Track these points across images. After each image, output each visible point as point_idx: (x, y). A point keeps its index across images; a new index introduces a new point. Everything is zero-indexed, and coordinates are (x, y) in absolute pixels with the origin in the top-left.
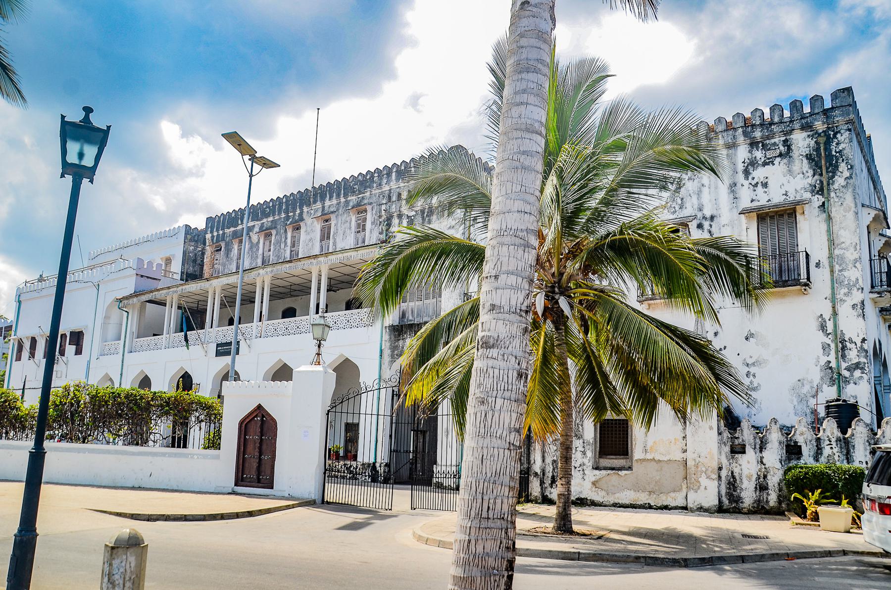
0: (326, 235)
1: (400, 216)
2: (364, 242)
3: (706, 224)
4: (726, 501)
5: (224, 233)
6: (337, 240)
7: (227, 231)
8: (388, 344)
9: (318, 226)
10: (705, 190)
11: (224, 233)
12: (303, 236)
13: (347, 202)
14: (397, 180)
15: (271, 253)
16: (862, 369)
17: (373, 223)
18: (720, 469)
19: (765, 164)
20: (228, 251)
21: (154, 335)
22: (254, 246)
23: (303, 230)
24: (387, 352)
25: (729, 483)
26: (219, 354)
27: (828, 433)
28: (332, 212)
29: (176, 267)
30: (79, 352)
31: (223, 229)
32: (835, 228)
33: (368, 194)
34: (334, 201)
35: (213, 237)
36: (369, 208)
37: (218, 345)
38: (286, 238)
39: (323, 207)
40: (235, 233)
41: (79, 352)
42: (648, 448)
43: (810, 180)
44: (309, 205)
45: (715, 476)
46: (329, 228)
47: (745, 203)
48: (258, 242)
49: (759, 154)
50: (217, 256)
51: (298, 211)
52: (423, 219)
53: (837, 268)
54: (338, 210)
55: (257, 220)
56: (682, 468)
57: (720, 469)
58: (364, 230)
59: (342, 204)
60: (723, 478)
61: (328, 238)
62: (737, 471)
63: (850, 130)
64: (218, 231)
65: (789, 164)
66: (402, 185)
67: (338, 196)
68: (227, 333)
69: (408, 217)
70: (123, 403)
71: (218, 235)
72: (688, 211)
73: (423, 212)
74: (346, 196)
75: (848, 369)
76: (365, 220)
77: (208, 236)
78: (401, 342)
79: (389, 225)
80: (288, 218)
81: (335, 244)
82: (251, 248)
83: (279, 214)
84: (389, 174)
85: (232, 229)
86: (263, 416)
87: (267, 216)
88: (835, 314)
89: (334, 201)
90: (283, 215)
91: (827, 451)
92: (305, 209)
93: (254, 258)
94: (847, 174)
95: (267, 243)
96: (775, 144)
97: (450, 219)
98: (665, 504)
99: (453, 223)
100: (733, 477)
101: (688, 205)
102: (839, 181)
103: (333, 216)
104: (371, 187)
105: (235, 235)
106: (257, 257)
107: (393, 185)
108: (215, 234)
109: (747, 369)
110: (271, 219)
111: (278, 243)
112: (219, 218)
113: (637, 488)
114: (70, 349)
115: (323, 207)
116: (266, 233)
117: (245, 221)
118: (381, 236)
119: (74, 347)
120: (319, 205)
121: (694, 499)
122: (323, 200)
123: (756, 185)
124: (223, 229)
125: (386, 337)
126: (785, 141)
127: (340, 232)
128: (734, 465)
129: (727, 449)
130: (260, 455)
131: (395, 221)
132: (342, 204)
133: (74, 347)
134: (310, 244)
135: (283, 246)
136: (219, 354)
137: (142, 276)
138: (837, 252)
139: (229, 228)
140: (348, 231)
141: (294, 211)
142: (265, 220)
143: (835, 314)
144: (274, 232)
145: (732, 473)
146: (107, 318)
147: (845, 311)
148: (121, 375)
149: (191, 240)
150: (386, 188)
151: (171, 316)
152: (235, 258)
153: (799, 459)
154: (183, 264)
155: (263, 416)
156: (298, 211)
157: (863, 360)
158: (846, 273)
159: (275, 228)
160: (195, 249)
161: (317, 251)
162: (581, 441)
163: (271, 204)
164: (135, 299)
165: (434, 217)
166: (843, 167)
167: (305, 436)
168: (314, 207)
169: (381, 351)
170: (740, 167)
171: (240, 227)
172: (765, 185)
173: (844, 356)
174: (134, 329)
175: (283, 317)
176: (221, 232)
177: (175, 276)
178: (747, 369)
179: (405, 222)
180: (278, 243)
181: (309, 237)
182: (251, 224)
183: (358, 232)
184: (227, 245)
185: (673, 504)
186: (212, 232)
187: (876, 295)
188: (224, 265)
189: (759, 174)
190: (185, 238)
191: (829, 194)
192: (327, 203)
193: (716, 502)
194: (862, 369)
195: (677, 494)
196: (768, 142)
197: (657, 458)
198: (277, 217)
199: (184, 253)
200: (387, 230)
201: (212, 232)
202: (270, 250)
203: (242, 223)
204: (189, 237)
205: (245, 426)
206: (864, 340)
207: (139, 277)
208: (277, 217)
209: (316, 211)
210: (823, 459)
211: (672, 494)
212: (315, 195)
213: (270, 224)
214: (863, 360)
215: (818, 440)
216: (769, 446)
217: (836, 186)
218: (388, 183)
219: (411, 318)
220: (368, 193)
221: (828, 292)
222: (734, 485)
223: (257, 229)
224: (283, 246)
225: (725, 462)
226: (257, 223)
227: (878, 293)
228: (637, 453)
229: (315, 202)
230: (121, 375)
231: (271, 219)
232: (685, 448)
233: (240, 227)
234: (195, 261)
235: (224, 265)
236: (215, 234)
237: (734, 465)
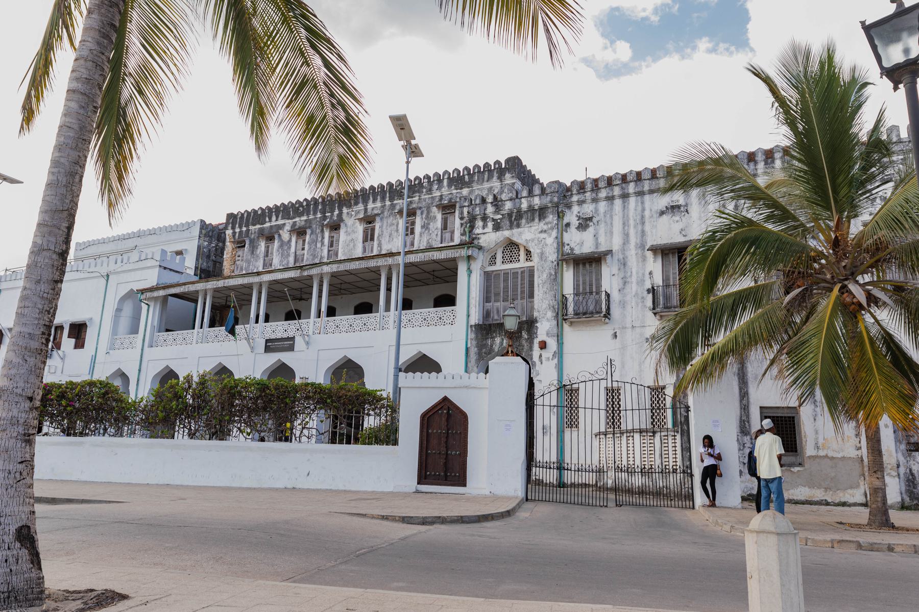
0: (369, 236)
1: (485, 218)
2: (412, 244)
4: (907, 499)
5: (248, 230)
6: (383, 242)
7: (251, 227)
8: (474, 343)
9: (360, 228)
11: (248, 230)
12: (343, 235)
13: (393, 206)
14: (449, 186)
15: (305, 252)
17: (423, 227)
18: (898, 466)
20: (254, 248)
21: (167, 330)
22: (285, 245)
23: (342, 231)
24: (473, 351)
25: (908, 480)
26: (268, 349)
28: (378, 215)
29: (190, 263)
30: (79, 345)
31: (247, 226)
33: (417, 198)
34: (378, 204)
35: (234, 233)
36: (418, 212)
37: (267, 341)
38: (323, 238)
39: (366, 210)
40: (261, 230)
41: (79, 345)
42: (820, 444)
44: (349, 206)
45: (895, 474)
46: (373, 230)
48: (290, 241)
50: (240, 253)
51: (337, 212)
52: (511, 222)
54: (383, 212)
55: (288, 219)
56: (857, 465)
57: (898, 466)
58: (412, 232)
59: (387, 207)
60: (902, 476)
61: (372, 239)
62: (915, 468)
64: (240, 227)
66: (455, 191)
67: (383, 199)
68: (280, 329)
69: (493, 220)
70: (272, 395)
71: (241, 232)
73: (510, 215)
74: (391, 199)
76: (413, 223)
77: (229, 232)
78: (489, 342)
79: (472, 227)
80: (325, 218)
81: (380, 245)
82: (281, 246)
83: (315, 213)
84: (440, 181)
85: (258, 226)
86: (449, 409)
87: (301, 215)
89: (378, 204)
90: (319, 215)
92: (345, 210)
93: (284, 256)
95: (300, 242)
97: (542, 224)
98: (843, 500)
99: (545, 227)
100: (912, 474)
103: (378, 219)
104: (420, 192)
105: (261, 233)
106: (289, 255)
107: (445, 191)
108: (237, 230)
110: (305, 218)
111: (314, 242)
112: (243, 215)
113: (811, 485)
114: (68, 343)
115: (366, 210)
116: (300, 232)
117: (274, 218)
118: (464, 238)
119: (73, 341)
120: (361, 207)
121: (847, 497)
122: (365, 202)
124: (247, 226)
125: (472, 335)
127: (386, 234)
128: (912, 462)
130: (447, 451)
131: (479, 223)
132: (387, 207)
133: (73, 341)
134: (352, 245)
135: (319, 245)
136: (268, 349)
137: (165, 268)
139: (254, 225)
141: (332, 212)
142: (297, 219)
144: (309, 231)
145: (911, 470)
146: (119, 310)
148: (140, 370)
149: (205, 235)
150: (438, 194)
151: (204, 309)
152: (262, 256)
154: (197, 259)
155: (449, 409)
156: (337, 212)
159: (310, 227)
160: (209, 245)
161: (359, 253)
162: (748, 437)
163: (305, 204)
164: (162, 293)
165: (524, 221)
167: (507, 430)
168: (355, 208)
169: (467, 349)
171: (267, 225)
174: (156, 324)
175: (356, 313)
176: (244, 229)
177: (188, 271)
179: (490, 225)
180: (314, 242)
181: (349, 238)
182: (280, 222)
183: (407, 235)
184: (252, 241)
185: (851, 500)
186: (233, 228)
188: (248, 262)
190: (201, 232)
192: (370, 205)
193: (899, 499)
195: (855, 491)
197: (830, 455)
198: (311, 217)
199: (199, 247)
200: (470, 232)
201: (233, 228)
202: (303, 249)
203: (270, 221)
204: (204, 232)
205: (428, 419)
207: (162, 269)
208: (311, 217)
209: (358, 212)
211: (850, 491)
212: (357, 197)
213: (303, 223)
218: (439, 188)
219: (496, 317)
220: (417, 198)
222: (913, 482)
223: (288, 227)
224: (319, 245)
225: (902, 459)
226: (287, 221)
228: (809, 450)
229: (356, 204)
230: (140, 370)
231: (305, 218)
232: (858, 445)
233: (267, 225)
234: (208, 257)
235: (248, 262)
236: (237, 230)
237: (912, 462)
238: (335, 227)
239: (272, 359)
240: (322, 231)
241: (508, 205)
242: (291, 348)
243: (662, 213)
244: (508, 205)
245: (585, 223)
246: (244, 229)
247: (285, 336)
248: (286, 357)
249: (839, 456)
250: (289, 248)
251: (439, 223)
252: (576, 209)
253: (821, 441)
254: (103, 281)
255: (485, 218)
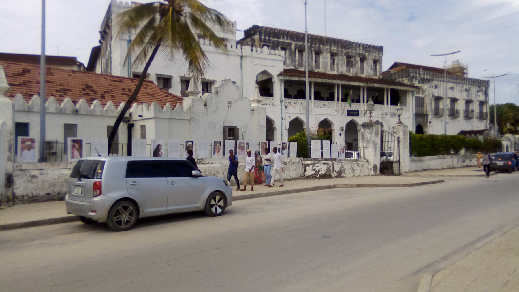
7: (272, 39)
11: (269, 40)
23: (321, 56)
37: (348, 111)
38: (312, 57)
44: (324, 45)
51: (317, 46)
55: (293, 41)
74: (341, 48)
85: (276, 39)
89: (336, 49)
124: (269, 37)
127: (340, 63)
131: (414, 80)
139: (274, 38)
140: (343, 65)
141: (316, 45)
156: (317, 46)
182: (289, 41)
203: (283, 38)
229: (327, 45)
238: (318, 53)
239: (350, 118)
240: (311, 53)
241: (422, 76)
242: (358, 115)
244: (422, 76)
245: (436, 87)
246: (267, 38)
247: (356, 109)
248: (356, 119)
250: (295, 57)
251: (359, 65)
252: (434, 82)
254: (240, 58)
255: (416, 78)
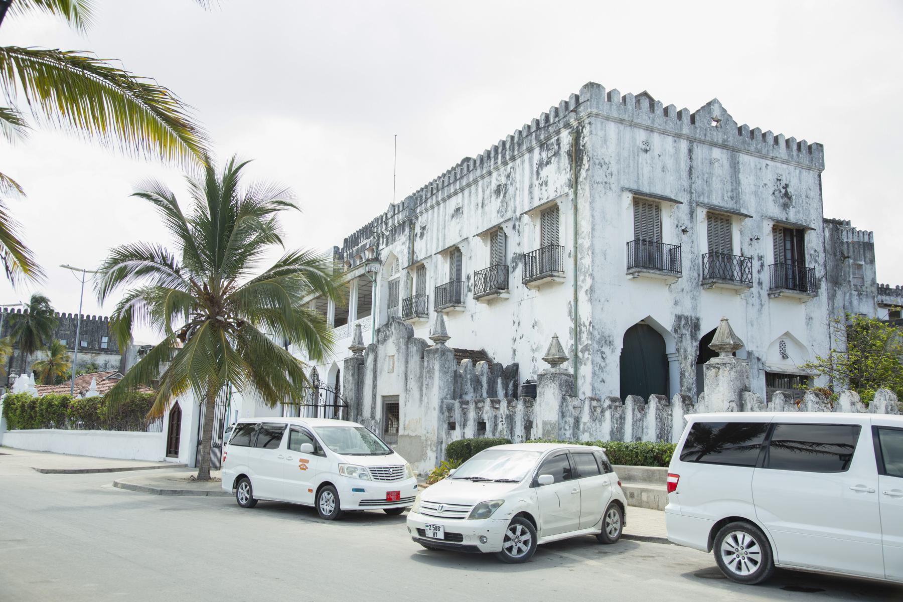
3: (517, 224)
10: (518, 192)
16: (589, 350)
18: (442, 443)
19: (547, 163)
27: (501, 411)
32: (579, 219)
43: (568, 176)
47: (536, 203)
49: (544, 155)
53: (579, 256)
63: (590, 123)
65: (559, 162)
72: (509, 215)
75: (582, 351)
88: (576, 299)
91: (500, 427)
94: (587, 166)
96: (552, 144)
101: (509, 208)
102: (583, 173)
109: (532, 355)
123: (541, 185)
126: (558, 140)
129: (446, 426)
138: (580, 241)
143: (576, 299)
147: (582, 297)
153: (484, 434)
157: (590, 342)
158: (583, 261)
166: (585, 158)
170: (535, 169)
172: (546, 183)
173: (580, 339)
178: (532, 355)
182: (365, 242)
187: (631, 277)
189: (544, 172)
191: (577, 187)
194: (589, 350)
196: (549, 142)
206: (590, 323)
210: (497, 434)
214: (590, 342)
215: (496, 416)
216: (468, 423)
217: (581, 179)
221: (573, 282)
225: (444, 436)
227: (632, 274)
233: (360, 245)
243: (453, 216)
249: (414, 435)
253: (407, 422)
